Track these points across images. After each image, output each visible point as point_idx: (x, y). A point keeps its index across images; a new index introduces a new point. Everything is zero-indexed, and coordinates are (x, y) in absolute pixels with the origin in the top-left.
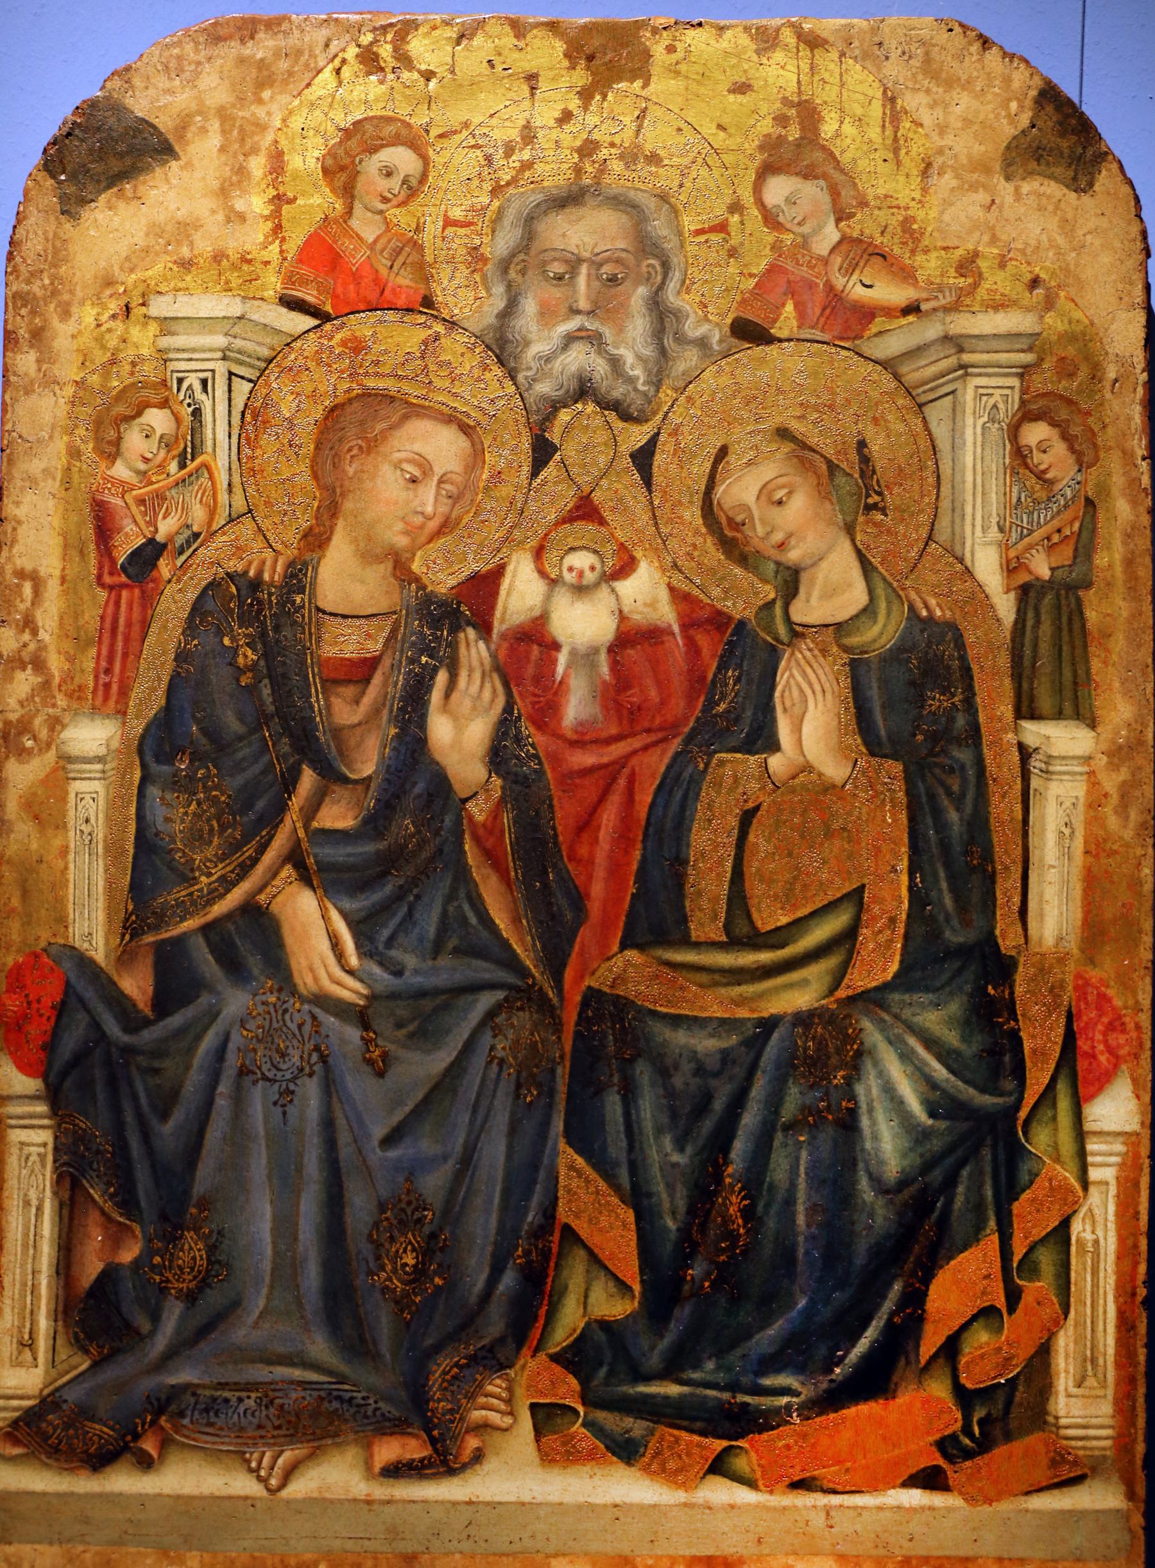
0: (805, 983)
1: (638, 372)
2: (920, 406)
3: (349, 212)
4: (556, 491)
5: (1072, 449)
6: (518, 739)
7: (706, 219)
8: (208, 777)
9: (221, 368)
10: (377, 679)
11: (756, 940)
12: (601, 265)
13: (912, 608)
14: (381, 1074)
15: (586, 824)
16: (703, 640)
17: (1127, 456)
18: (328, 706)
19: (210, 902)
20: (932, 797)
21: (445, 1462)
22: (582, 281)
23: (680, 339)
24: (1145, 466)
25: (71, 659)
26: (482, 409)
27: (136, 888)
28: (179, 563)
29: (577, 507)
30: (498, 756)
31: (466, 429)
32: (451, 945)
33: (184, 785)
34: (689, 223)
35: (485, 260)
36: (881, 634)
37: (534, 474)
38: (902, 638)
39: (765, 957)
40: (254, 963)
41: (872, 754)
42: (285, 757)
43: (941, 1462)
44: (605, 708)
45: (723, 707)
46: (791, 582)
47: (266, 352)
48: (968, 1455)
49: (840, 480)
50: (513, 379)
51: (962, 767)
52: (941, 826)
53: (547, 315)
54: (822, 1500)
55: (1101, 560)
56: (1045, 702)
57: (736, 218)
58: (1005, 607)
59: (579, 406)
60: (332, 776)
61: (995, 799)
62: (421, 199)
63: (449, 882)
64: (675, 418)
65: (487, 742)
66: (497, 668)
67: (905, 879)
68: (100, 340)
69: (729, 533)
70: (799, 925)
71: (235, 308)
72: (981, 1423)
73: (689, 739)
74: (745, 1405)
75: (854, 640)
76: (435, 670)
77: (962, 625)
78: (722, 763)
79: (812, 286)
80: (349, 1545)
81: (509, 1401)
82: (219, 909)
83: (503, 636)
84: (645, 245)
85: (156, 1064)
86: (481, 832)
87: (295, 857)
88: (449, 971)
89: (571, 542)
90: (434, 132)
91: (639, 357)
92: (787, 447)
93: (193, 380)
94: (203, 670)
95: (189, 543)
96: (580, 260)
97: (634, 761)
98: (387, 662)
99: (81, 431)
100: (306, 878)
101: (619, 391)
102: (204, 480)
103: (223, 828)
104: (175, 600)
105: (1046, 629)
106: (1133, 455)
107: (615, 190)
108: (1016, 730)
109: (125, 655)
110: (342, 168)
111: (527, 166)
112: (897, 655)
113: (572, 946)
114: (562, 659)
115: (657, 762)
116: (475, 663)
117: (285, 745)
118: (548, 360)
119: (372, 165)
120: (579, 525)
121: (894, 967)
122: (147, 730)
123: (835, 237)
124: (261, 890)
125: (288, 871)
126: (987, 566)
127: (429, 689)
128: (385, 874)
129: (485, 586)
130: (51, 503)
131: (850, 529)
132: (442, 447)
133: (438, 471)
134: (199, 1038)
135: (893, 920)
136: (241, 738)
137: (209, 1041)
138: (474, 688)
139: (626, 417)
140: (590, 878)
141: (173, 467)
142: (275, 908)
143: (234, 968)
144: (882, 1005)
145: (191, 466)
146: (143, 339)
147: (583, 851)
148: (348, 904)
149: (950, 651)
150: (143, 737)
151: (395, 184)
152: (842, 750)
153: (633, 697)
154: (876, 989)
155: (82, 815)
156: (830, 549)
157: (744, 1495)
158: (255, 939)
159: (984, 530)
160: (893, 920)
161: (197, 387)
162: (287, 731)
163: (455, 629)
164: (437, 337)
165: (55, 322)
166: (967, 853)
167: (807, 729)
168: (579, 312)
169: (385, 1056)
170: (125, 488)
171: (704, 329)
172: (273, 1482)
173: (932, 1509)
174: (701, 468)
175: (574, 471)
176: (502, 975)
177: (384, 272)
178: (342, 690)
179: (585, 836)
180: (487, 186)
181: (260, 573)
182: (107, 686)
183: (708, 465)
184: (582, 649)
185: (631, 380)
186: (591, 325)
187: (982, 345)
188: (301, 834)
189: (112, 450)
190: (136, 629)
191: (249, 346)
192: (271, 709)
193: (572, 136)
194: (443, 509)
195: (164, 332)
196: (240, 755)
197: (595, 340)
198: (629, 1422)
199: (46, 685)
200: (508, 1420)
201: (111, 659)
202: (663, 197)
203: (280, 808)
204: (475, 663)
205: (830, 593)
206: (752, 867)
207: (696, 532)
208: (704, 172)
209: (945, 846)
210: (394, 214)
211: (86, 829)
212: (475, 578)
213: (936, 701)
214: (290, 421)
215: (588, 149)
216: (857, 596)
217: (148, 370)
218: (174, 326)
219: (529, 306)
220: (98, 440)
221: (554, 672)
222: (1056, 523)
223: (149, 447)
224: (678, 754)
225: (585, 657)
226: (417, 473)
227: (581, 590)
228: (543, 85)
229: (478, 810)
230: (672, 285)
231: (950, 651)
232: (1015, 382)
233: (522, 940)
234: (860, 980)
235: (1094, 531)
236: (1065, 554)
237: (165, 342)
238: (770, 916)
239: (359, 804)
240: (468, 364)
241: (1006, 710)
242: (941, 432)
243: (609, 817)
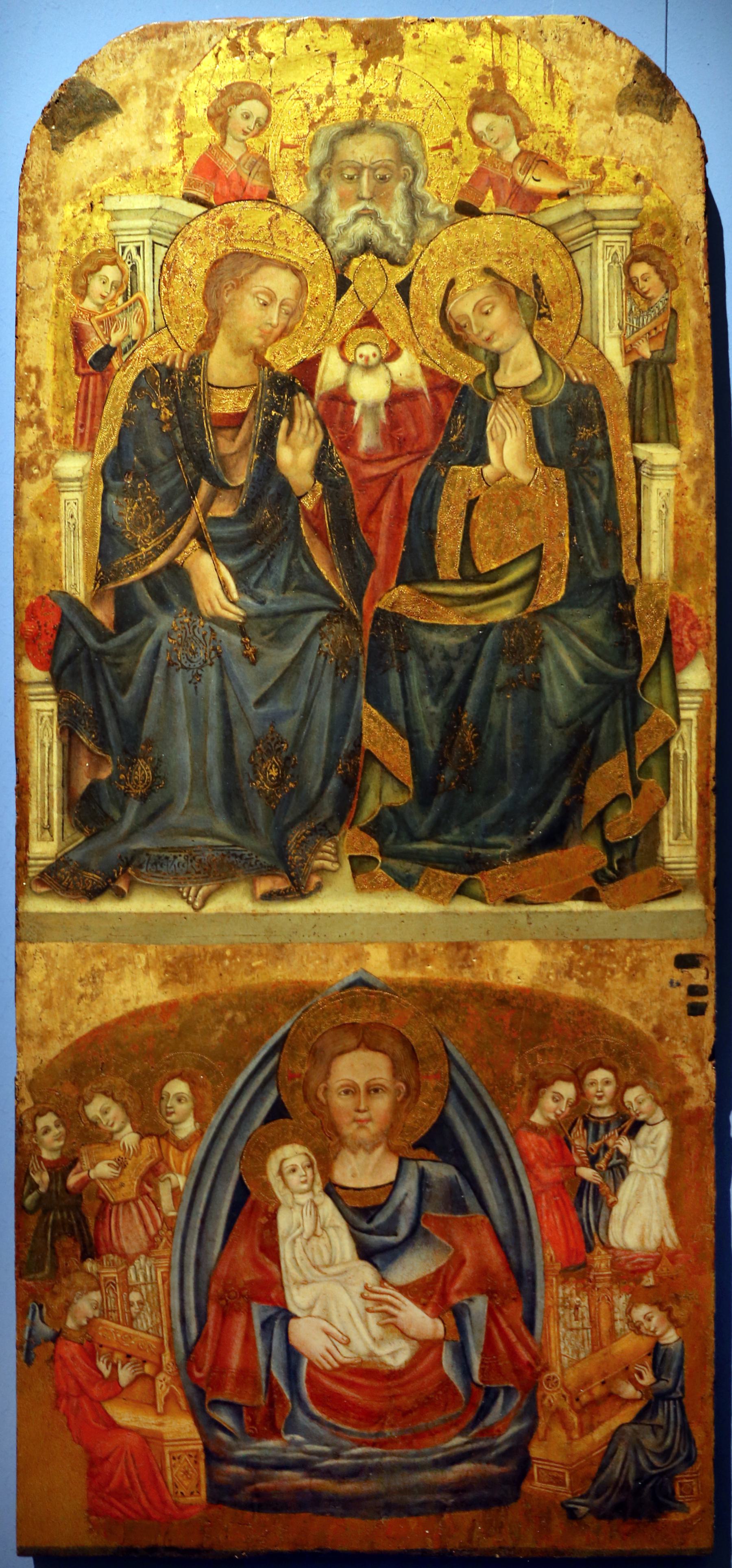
0: (507, 604)
1: (400, 235)
2: (571, 253)
3: (224, 141)
4: (351, 309)
5: (662, 279)
6: (332, 460)
7: (440, 140)
8: (144, 487)
9: (148, 240)
10: (246, 425)
11: (479, 578)
12: (375, 170)
13: (568, 376)
14: (253, 663)
15: (374, 510)
16: (442, 398)
17: (695, 283)
18: (216, 443)
19: (148, 563)
20: (582, 490)
21: (299, 891)
22: (364, 180)
23: (425, 214)
24: (706, 289)
25: (60, 420)
26: (306, 261)
27: (101, 555)
28: (124, 358)
29: (364, 318)
30: (319, 470)
31: (296, 272)
32: (294, 585)
33: (130, 493)
34: (429, 143)
35: (305, 168)
36: (550, 392)
37: (338, 298)
38: (563, 395)
39: (484, 588)
40: (175, 598)
41: (546, 465)
42: (191, 474)
43: (595, 885)
44: (384, 440)
45: (455, 438)
46: (494, 361)
47: (175, 229)
48: (611, 880)
49: (523, 299)
50: (324, 240)
51: (600, 473)
52: (588, 508)
53: (344, 201)
54: (525, 908)
55: (681, 346)
56: (649, 433)
57: (456, 140)
58: (624, 374)
59: (364, 257)
60: (219, 485)
61: (620, 491)
62: (267, 132)
63: (292, 545)
64: (422, 263)
65: (313, 461)
66: (318, 417)
67: (567, 540)
68: (75, 226)
69: (456, 332)
70: (503, 569)
71: (156, 202)
72: (619, 862)
73: (435, 458)
74: (478, 855)
75: (533, 396)
76: (280, 419)
77: (600, 386)
78: (455, 472)
79: (503, 180)
80: (244, 939)
81: (336, 855)
82: (152, 567)
83: (321, 398)
84: (403, 157)
85: (118, 661)
86: (310, 516)
87: (198, 534)
88: (293, 600)
89: (362, 339)
90: (274, 91)
91: (400, 226)
92: (490, 280)
93: (131, 248)
94: (140, 423)
95: (130, 347)
96: (363, 167)
97: (402, 471)
98: (251, 415)
99: (65, 282)
100: (205, 546)
101: (388, 247)
102: (139, 308)
103: (154, 518)
104: (123, 381)
105: (649, 387)
106: (698, 283)
107: (383, 124)
108: (632, 449)
109: (93, 416)
110: (220, 115)
111: (330, 110)
112: (559, 405)
113: (366, 582)
114: (357, 410)
115: (416, 473)
116: (305, 414)
117: (190, 467)
118: (345, 228)
119: (237, 112)
120: (365, 329)
121: (561, 593)
122: (107, 460)
123: (517, 150)
124: (178, 555)
125: (194, 543)
126: (613, 350)
127: (277, 431)
128: (251, 544)
129: (309, 368)
130: (47, 326)
131: (530, 329)
132: (282, 283)
133: (280, 298)
134: (143, 644)
135: (560, 565)
136: (163, 464)
137: (149, 646)
138: (304, 430)
139: (393, 262)
140: (377, 542)
141: (120, 301)
142: (186, 565)
143: (163, 602)
144: (555, 616)
145: (131, 300)
146: (100, 223)
147: (372, 526)
148: (231, 562)
149: (591, 402)
150: (104, 465)
151: (251, 123)
152: (527, 463)
153: (401, 433)
154: (552, 606)
155: (69, 513)
156: (518, 341)
157: (478, 907)
158: (174, 584)
159: (611, 328)
160: (560, 565)
161: (134, 252)
162: (192, 458)
163: (292, 394)
164: (278, 216)
165: (48, 215)
166: (604, 524)
167: (506, 450)
168: (363, 199)
169: (255, 652)
170: (91, 314)
171: (439, 208)
172: (197, 904)
173: (590, 912)
174: (438, 293)
175: (362, 296)
176: (325, 602)
177: (245, 177)
178: (224, 432)
179: (373, 519)
180: (307, 123)
181: (173, 363)
182: (82, 435)
183: (443, 291)
184: (369, 404)
185: (396, 240)
186: (371, 207)
187: (606, 216)
188: (201, 520)
189: (82, 292)
190: (99, 401)
191: (165, 226)
192: (182, 445)
193: (357, 90)
194: (283, 321)
195: (114, 219)
196: (163, 474)
197: (373, 215)
198: (408, 865)
199: (46, 435)
200: (336, 866)
201: (84, 419)
202: (413, 127)
203: (189, 505)
204: (305, 414)
205: (519, 368)
206: (475, 534)
207: (437, 332)
208: (437, 111)
209: (591, 519)
210: (251, 141)
211: (72, 521)
212: (304, 363)
213: (584, 433)
214: (190, 270)
215: (367, 98)
216: (535, 369)
217: (105, 243)
218: (119, 215)
219: (333, 196)
220: (74, 286)
221: (352, 419)
222: (653, 324)
223: (105, 290)
224: (428, 467)
225: (371, 409)
226: (267, 300)
227: (368, 368)
228: (339, 60)
229: (308, 503)
230: (419, 181)
231: (591, 402)
232: (627, 238)
233: (337, 582)
234: (542, 601)
235: (676, 328)
236: (660, 343)
237: (114, 225)
238: (486, 563)
239: (236, 501)
240: (297, 233)
241: (626, 438)
242: (583, 269)
243: (388, 506)
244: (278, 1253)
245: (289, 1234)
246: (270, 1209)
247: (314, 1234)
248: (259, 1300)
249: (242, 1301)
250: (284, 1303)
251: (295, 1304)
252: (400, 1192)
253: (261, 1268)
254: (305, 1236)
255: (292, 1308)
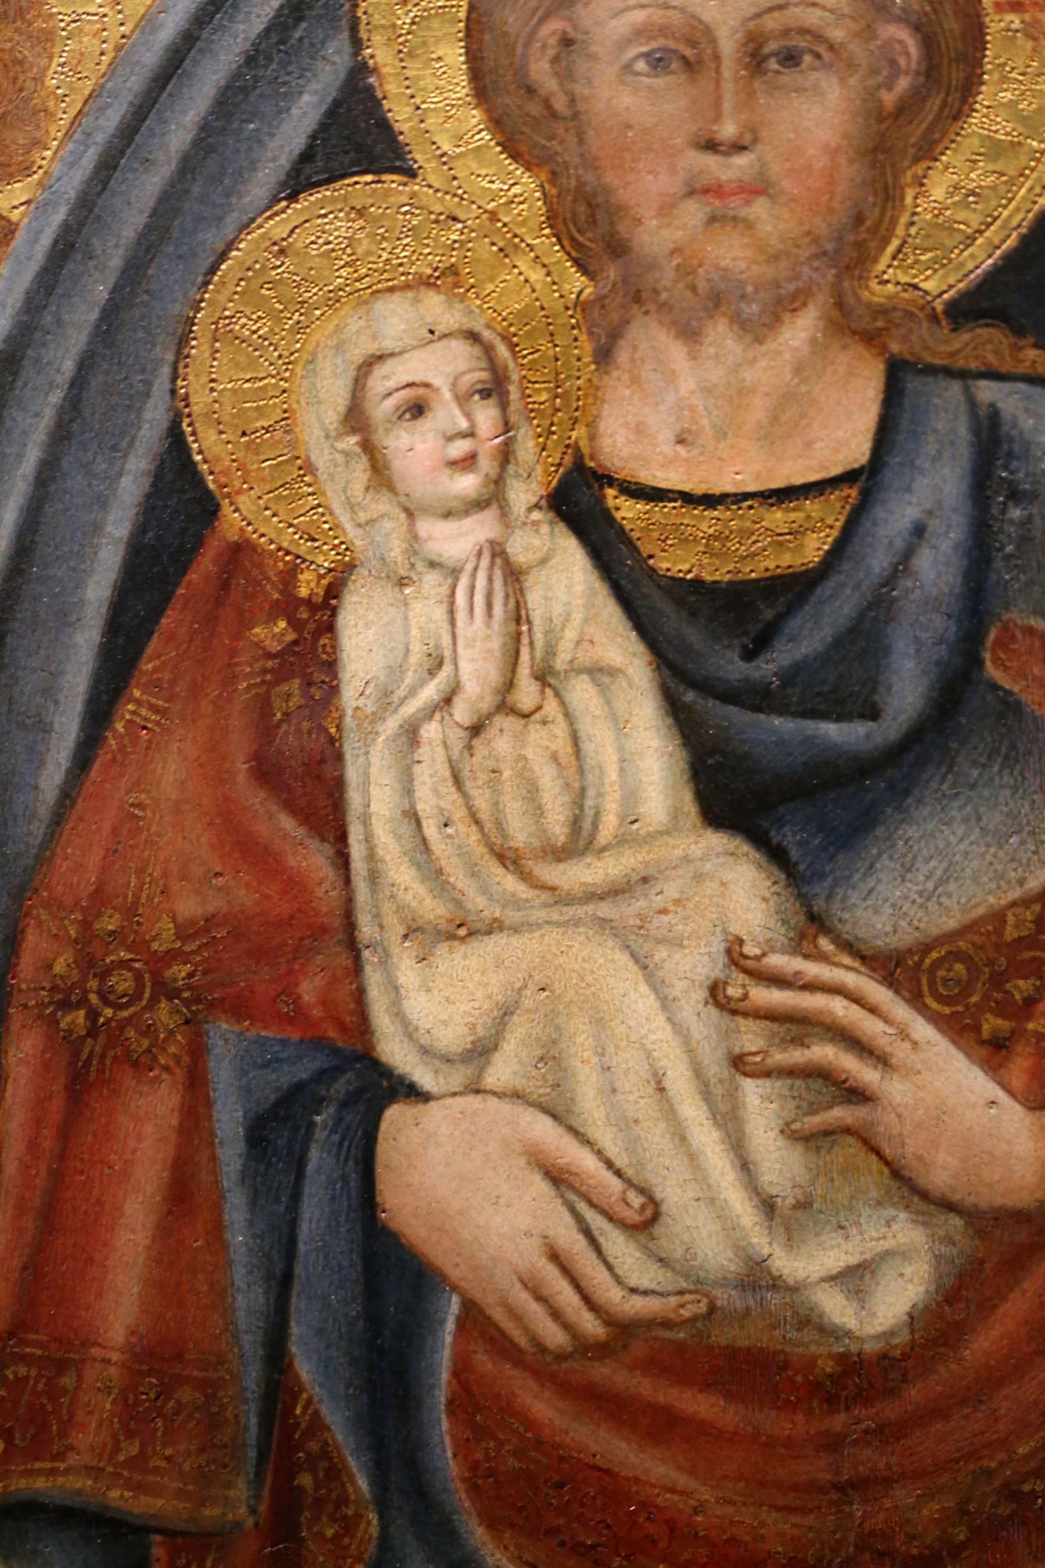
244: (335, 791)
245: (387, 701)
246: (307, 585)
247: (504, 706)
248: (239, 1009)
249: (164, 1014)
250: (362, 1025)
251: (409, 1031)
252: (897, 516)
253: (255, 854)
254: (462, 713)
255: (395, 1052)
